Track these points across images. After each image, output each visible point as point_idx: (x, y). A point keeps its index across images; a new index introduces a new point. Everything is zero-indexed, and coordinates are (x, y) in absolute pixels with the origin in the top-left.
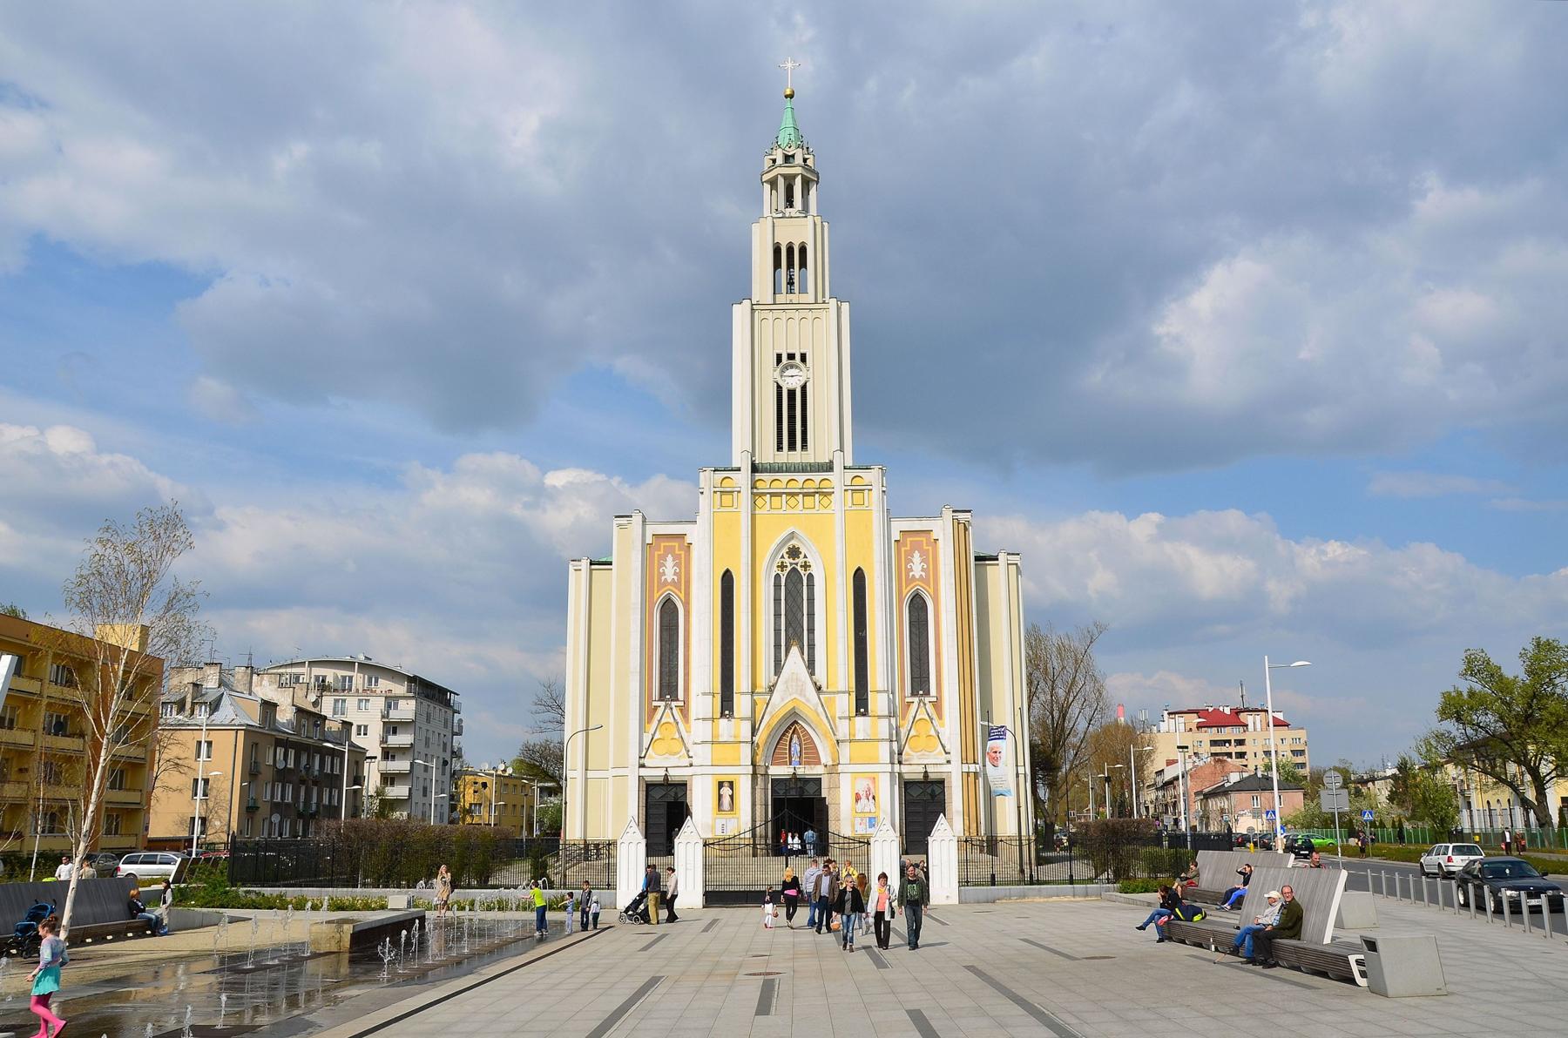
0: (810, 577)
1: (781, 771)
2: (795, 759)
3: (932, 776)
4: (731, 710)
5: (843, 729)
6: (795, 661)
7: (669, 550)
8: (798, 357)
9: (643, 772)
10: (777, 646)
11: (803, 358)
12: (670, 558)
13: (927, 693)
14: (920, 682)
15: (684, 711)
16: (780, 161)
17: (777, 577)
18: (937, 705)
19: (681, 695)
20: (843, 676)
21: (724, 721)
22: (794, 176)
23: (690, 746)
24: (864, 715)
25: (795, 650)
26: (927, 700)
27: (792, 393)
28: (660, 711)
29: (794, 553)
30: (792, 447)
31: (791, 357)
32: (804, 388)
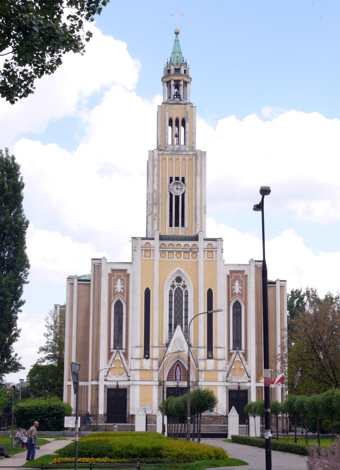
0: (187, 292)
1: (171, 384)
2: (178, 378)
3: (242, 388)
4: (149, 354)
5: (202, 365)
6: (179, 332)
7: (119, 277)
8: (180, 179)
9: (107, 383)
10: (170, 325)
11: (183, 179)
12: (119, 281)
13: (240, 349)
14: (237, 343)
15: (126, 355)
16: (172, 72)
17: (171, 292)
18: (245, 355)
19: (124, 346)
20: (203, 341)
21: (145, 360)
22: (179, 81)
23: (128, 370)
24: (211, 358)
25: (179, 327)
26: (240, 352)
27: (177, 198)
28: (114, 354)
29: (179, 279)
30: (177, 225)
31: (177, 179)
32: (183, 195)
